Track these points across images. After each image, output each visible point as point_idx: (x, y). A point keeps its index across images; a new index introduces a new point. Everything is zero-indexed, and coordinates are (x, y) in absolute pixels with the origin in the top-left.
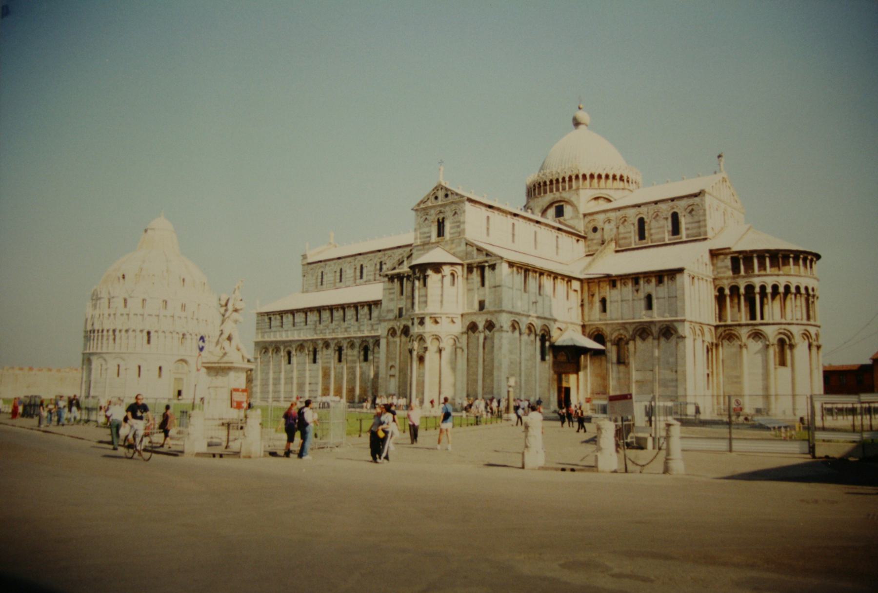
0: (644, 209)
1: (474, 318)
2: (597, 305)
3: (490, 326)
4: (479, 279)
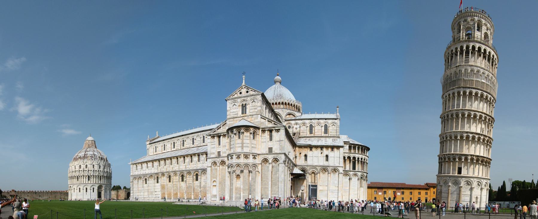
0: (312, 121)
3: (276, 160)
4: (268, 137)
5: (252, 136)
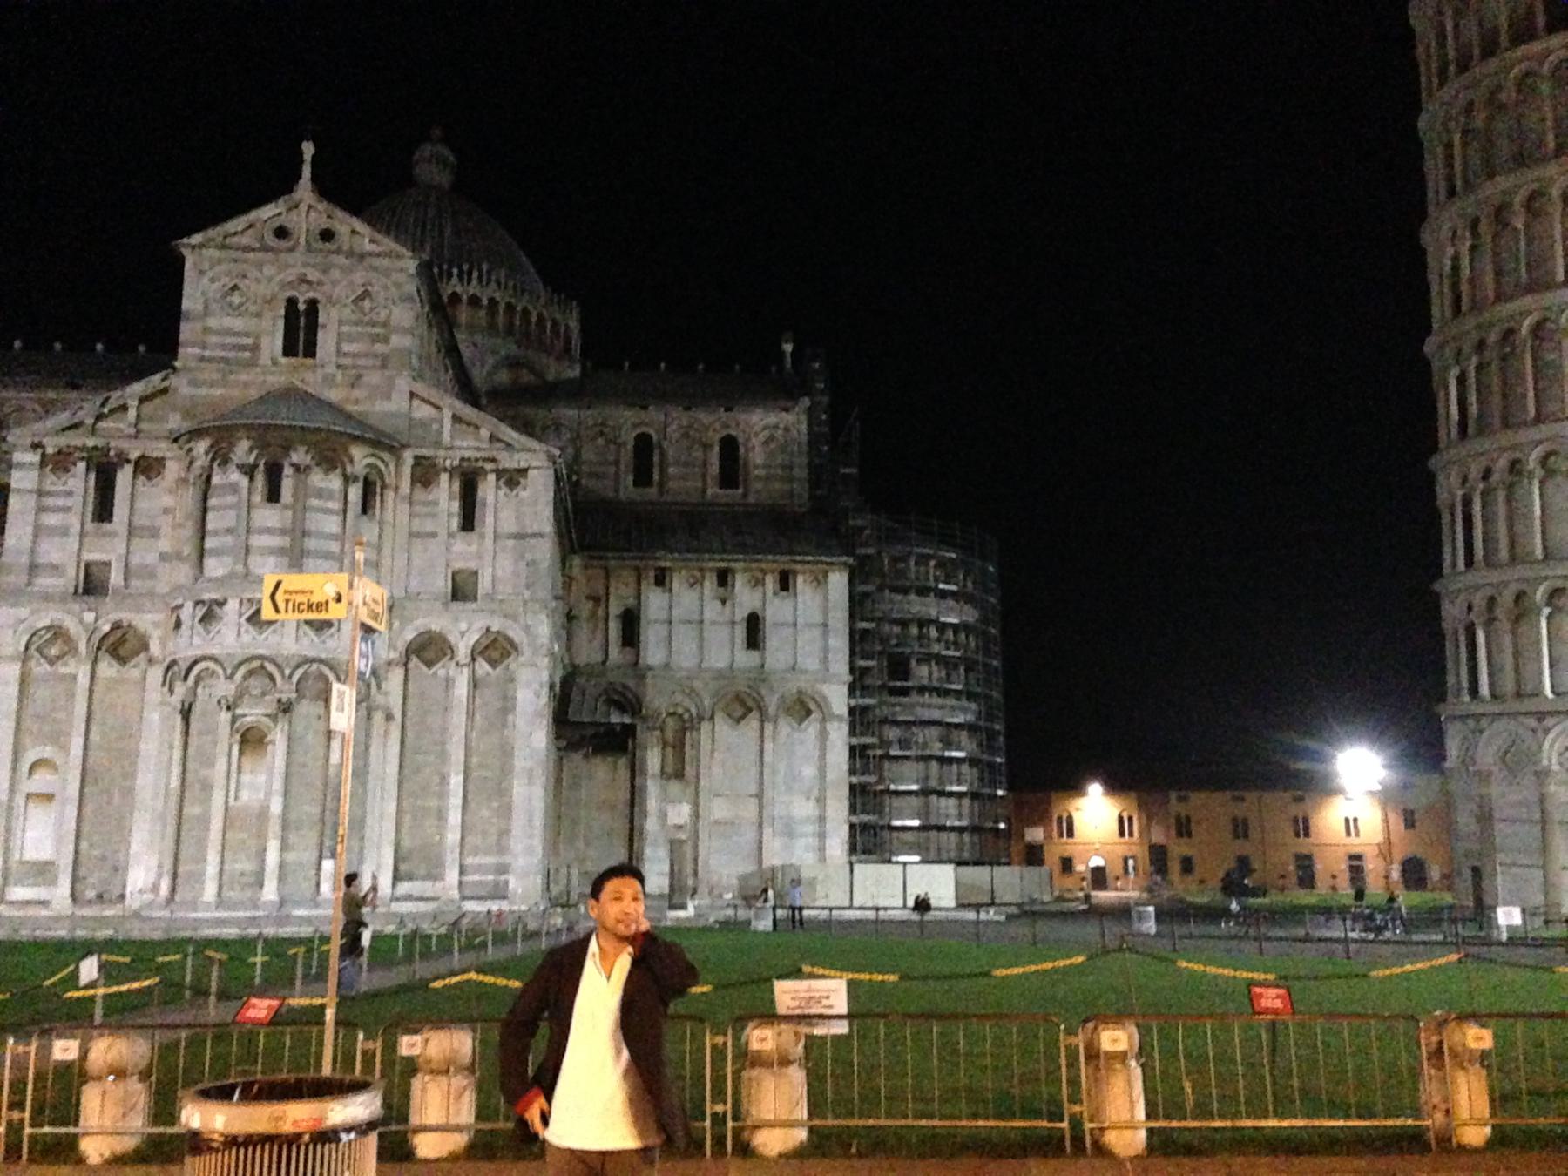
1: (437, 622)
2: (614, 628)
3: (495, 649)
4: (456, 506)
5: (355, 493)
